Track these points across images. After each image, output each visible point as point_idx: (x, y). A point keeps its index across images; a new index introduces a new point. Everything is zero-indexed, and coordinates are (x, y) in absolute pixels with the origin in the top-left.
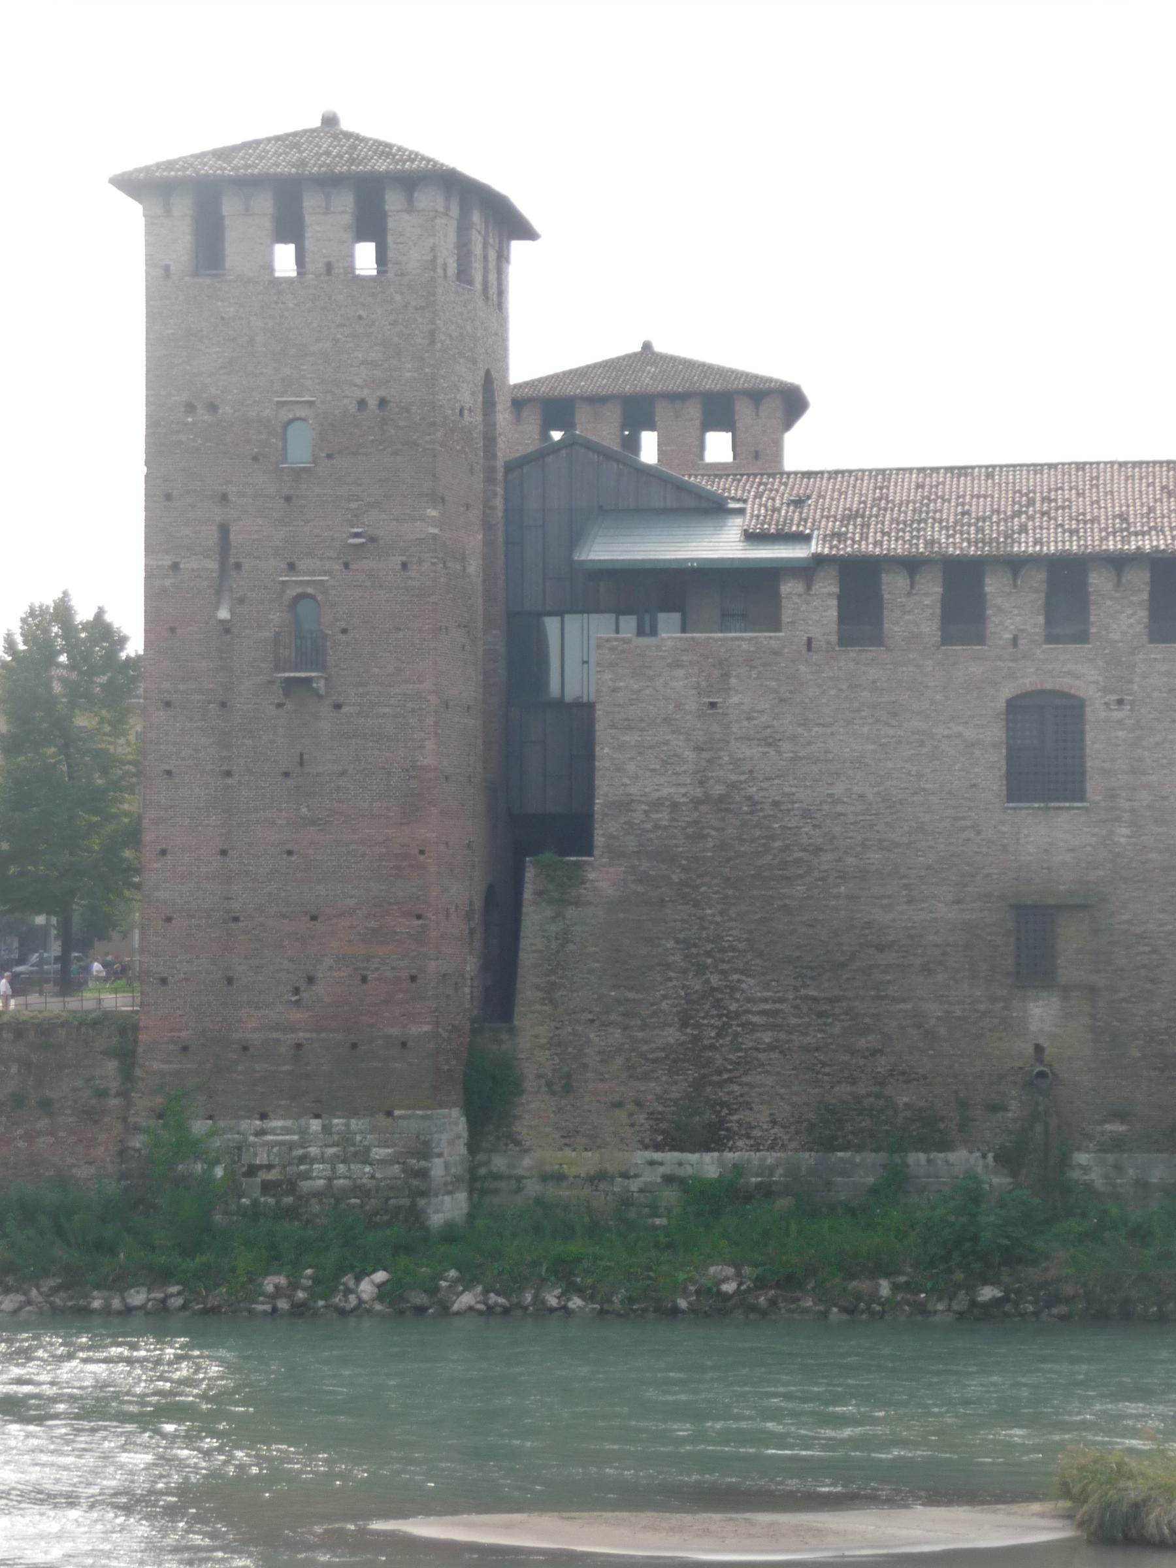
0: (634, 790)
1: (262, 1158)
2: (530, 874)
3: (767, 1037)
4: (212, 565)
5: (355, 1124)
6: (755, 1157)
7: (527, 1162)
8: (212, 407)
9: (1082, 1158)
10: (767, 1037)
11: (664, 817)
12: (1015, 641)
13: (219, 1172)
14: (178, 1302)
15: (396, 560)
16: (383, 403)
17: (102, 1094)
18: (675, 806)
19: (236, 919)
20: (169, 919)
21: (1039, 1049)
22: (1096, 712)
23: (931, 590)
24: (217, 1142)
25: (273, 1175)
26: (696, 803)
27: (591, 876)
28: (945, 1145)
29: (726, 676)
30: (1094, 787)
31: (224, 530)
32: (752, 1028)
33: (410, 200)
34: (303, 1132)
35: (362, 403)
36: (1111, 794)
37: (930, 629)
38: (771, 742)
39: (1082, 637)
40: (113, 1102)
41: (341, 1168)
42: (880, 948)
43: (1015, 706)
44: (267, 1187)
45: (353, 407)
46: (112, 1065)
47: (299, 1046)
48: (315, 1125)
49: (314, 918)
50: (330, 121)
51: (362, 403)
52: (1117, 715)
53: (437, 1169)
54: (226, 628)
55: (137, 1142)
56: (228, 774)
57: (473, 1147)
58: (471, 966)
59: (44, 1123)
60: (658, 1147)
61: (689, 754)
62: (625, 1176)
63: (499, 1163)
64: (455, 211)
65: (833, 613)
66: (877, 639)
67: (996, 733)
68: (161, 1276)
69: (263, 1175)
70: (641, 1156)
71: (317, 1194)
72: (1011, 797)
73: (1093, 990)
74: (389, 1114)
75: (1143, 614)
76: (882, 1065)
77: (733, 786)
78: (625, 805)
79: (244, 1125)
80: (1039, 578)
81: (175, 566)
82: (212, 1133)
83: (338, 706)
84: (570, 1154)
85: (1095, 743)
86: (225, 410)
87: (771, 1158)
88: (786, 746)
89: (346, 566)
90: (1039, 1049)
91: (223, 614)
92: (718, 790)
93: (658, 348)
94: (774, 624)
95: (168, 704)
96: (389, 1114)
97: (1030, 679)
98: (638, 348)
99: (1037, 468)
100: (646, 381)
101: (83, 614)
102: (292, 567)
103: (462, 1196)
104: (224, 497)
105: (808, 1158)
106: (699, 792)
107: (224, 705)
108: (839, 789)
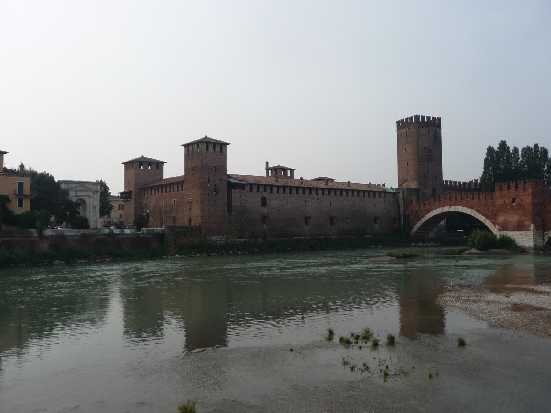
1: (213, 241)
5: (221, 237)
6: (245, 239)
7: (229, 240)
8: (208, 165)
9: (268, 238)
10: (246, 228)
14: (217, 254)
15: (223, 181)
16: (222, 165)
17: (198, 234)
18: (238, 206)
19: (210, 216)
20: (204, 216)
21: (265, 229)
22: (267, 199)
28: (259, 238)
30: (267, 205)
31: (209, 177)
33: (225, 146)
34: (216, 238)
36: (268, 206)
37: (256, 190)
40: (199, 235)
44: (214, 243)
45: (220, 165)
46: (198, 231)
48: (218, 237)
49: (216, 216)
50: (206, 136)
51: (221, 165)
52: (269, 199)
54: (209, 187)
56: (209, 202)
59: (192, 237)
60: (238, 239)
61: (239, 201)
62: (236, 241)
65: (249, 188)
67: (260, 200)
68: (215, 252)
70: (237, 240)
71: (219, 244)
72: (262, 206)
74: (224, 236)
75: (270, 190)
81: (204, 180)
82: (209, 238)
83: (218, 195)
86: (209, 165)
87: (247, 239)
88: (246, 201)
90: (265, 229)
91: (209, 185)
92: (241, 205)
93: (144, 156)
95: (204, 194)
96: (224, 236)
97: (263, 196)
98: (141, 156)
99: (237, 175)
100: (142, 160)
102: (215, 181)
107: (209, 195)
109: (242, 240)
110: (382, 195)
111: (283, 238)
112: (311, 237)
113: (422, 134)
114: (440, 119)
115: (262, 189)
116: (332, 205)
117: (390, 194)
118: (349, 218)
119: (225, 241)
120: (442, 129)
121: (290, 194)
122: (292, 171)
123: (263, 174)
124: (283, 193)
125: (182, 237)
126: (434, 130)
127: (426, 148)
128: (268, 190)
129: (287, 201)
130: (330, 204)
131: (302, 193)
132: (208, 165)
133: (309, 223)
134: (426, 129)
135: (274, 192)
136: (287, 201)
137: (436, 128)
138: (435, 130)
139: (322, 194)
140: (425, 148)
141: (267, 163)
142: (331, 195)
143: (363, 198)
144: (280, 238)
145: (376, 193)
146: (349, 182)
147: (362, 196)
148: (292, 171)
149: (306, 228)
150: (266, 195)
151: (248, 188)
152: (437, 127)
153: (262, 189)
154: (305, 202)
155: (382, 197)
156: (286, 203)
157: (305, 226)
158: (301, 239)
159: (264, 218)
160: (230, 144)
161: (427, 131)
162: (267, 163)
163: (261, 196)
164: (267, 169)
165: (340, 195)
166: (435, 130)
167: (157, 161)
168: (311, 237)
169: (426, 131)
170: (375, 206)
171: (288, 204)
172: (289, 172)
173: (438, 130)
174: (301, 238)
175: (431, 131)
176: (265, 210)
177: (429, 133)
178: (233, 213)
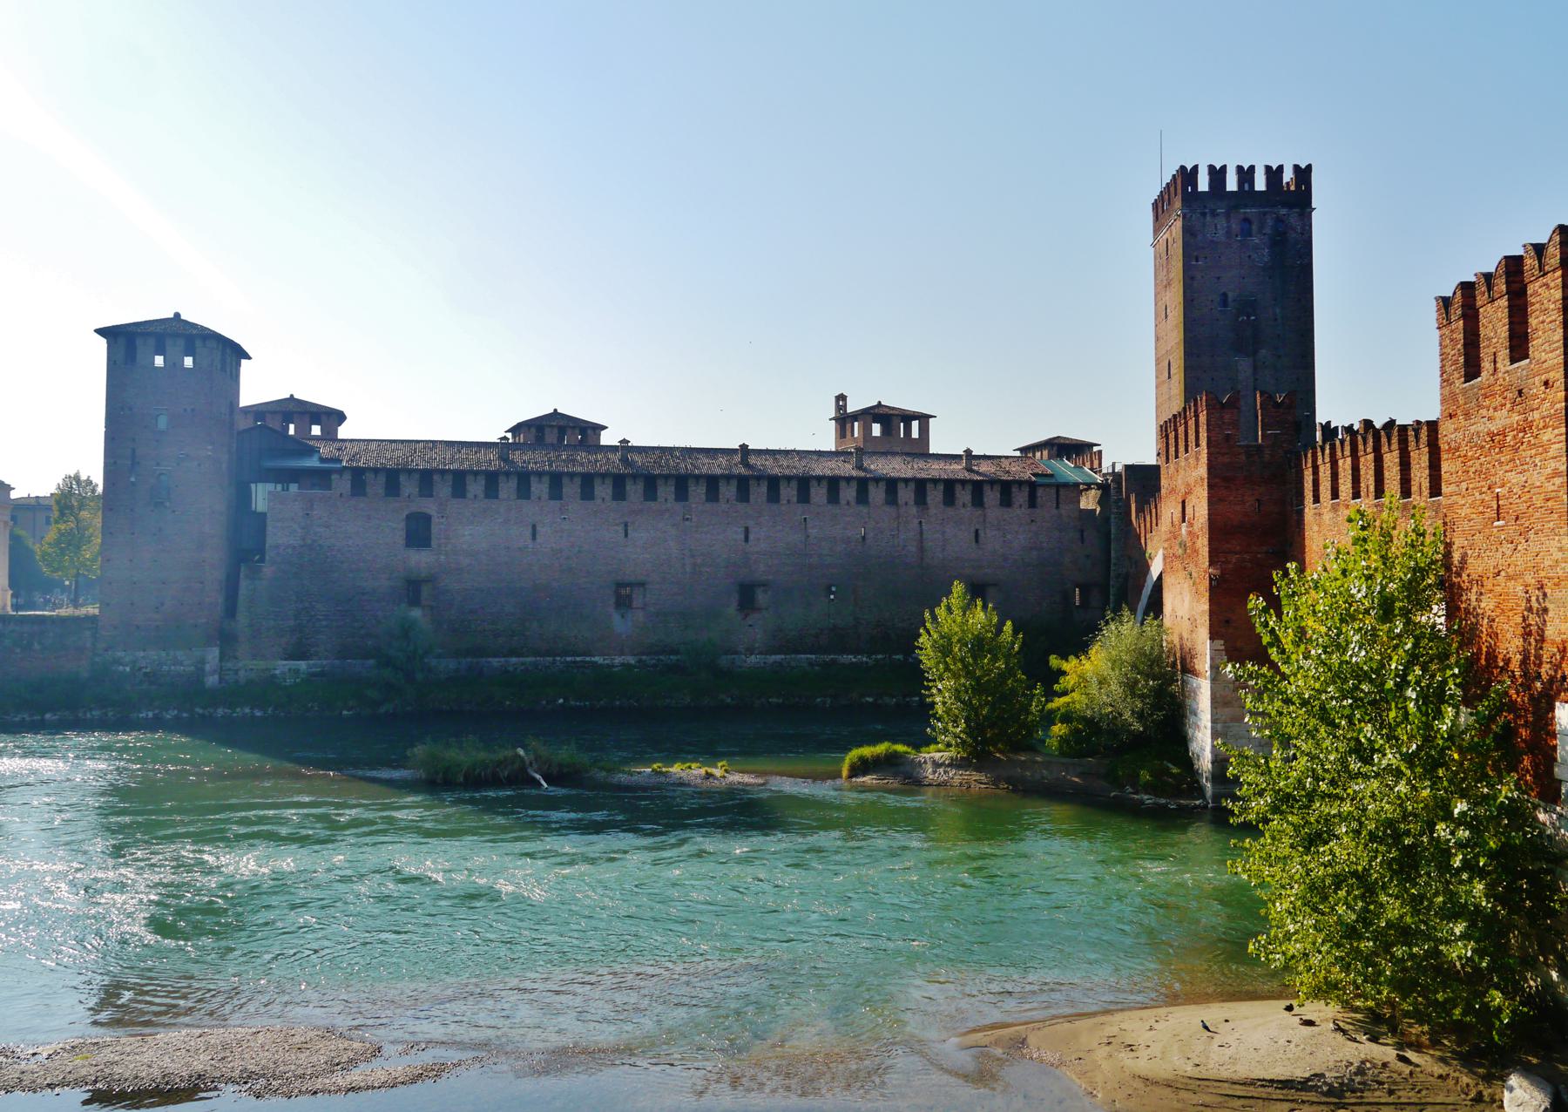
0: (280, 542)
2: (242, 569)
3: (324, 623)
4: (129, 463)
7: (240, 665)
10: (324, 623)
11: (290, 551)
12: (409, 496)
13: (128, 669)
16: (193, 410)
18: (294, 547)
22: (435, 520)
23: (382, 479)
24: (127, 659)
25: (148, 670)
26: (302, 546)
27: (265, 570)
29: (312, 505)
30: (434, 543)
32: (319, 620)
35: (185, 410)
36: (439, 546)
37: (381, 491)
38: (327, 527)
39: (431, 496)
41: (173, 668)
42: (363, 594)
43: (408, 517)
47: (157, 626)
50: (177, 315)
51: (185, 410)
53: (207, 667)
54: (133, 483)
55: (97, 659)
57: (221, 660)
58: (221, 600)
60: (286, 659)
61: (299, 531)
63: (229, 665)
64: (220, 348)
65: (349, 486)
66: (365, 494)
67: (403, 525)
69: (144, 670)
73: (432, 608)
75: (450, 489)
76: (362, 632)
77: (314, 541)
78: (277, 547)
79: (137, 654)
80: (417, 476)
81: (115, 463)
83: (174, 511)
84: (255, 662)
85: (434, 529)
87: (325, 662)
89: (178, 464)
91: (133, 479)
92: (309, 542)
93: (296, 397)
94: (329, 488)
97: (414, 508)
100: (291, 406)
101: (83, 477)
103: (216, 677)
104: (134, 440)
105: (337, 662)
106: (302, 543)
107: (132, 510)
108: (350, 542)
109: (303, 665)
110: (1020, 497)
111: (502, 659)
112: (644, 657)
113: (1212, 241)
114: (1303, 174)
115: (409, 487)
116: (751, 537)
117: (1062, 492)
118: (834, 589)
119: (192, 668)
120: (1314, 214)
121: (552, 502)
122: (924, 419)
123: (826, 439)
124: (514, 496)
125: (18, 650)
126: (1270, 222)
127: (1230, 300)
128: (443, 489)
129: (534, 527)
130: (742, 536)
131: (608, 498)
132: (130, 409)
133: (635, 604)
134: (1228, 222)
135: (470, 495)
136: (534, 527)
137: (1283, 211)
138: (1279, 220)
139: (703, 497)
140: (1225, 295)
141: (841, 398)
142: (751, 497)
143: (914, 510)
144: (490, 659)
145: (987, 488)
146: (744, 447)
147: (912, 502)
148: (924, 419)
149: (621, 625)
150: (428, 506)
151: (343, 485)
152: (1290, 206)
153: (409, 487)
154: (621, 529)
155: (1017, 504)
156: (528, 532)
157: (616, 618)
158: (596, 662)
159: (413, 588)
160: (97, 331)
161: (1235, 226)
162: (841, 398)
163: (406, 512)
164: (844, 420)
165: (795, 499)
166: (1279, 220)
167: (315, 410)
168: (644, 657)
169: (1229, 227)
170: (977, 541)
171: (537, 536)
172: (915, 424)
173: (1293, 220)
174: (596, 659)
175: (1254, 227)
176: (420, 560)
177: (1247, 233)
178: (268, 570)
